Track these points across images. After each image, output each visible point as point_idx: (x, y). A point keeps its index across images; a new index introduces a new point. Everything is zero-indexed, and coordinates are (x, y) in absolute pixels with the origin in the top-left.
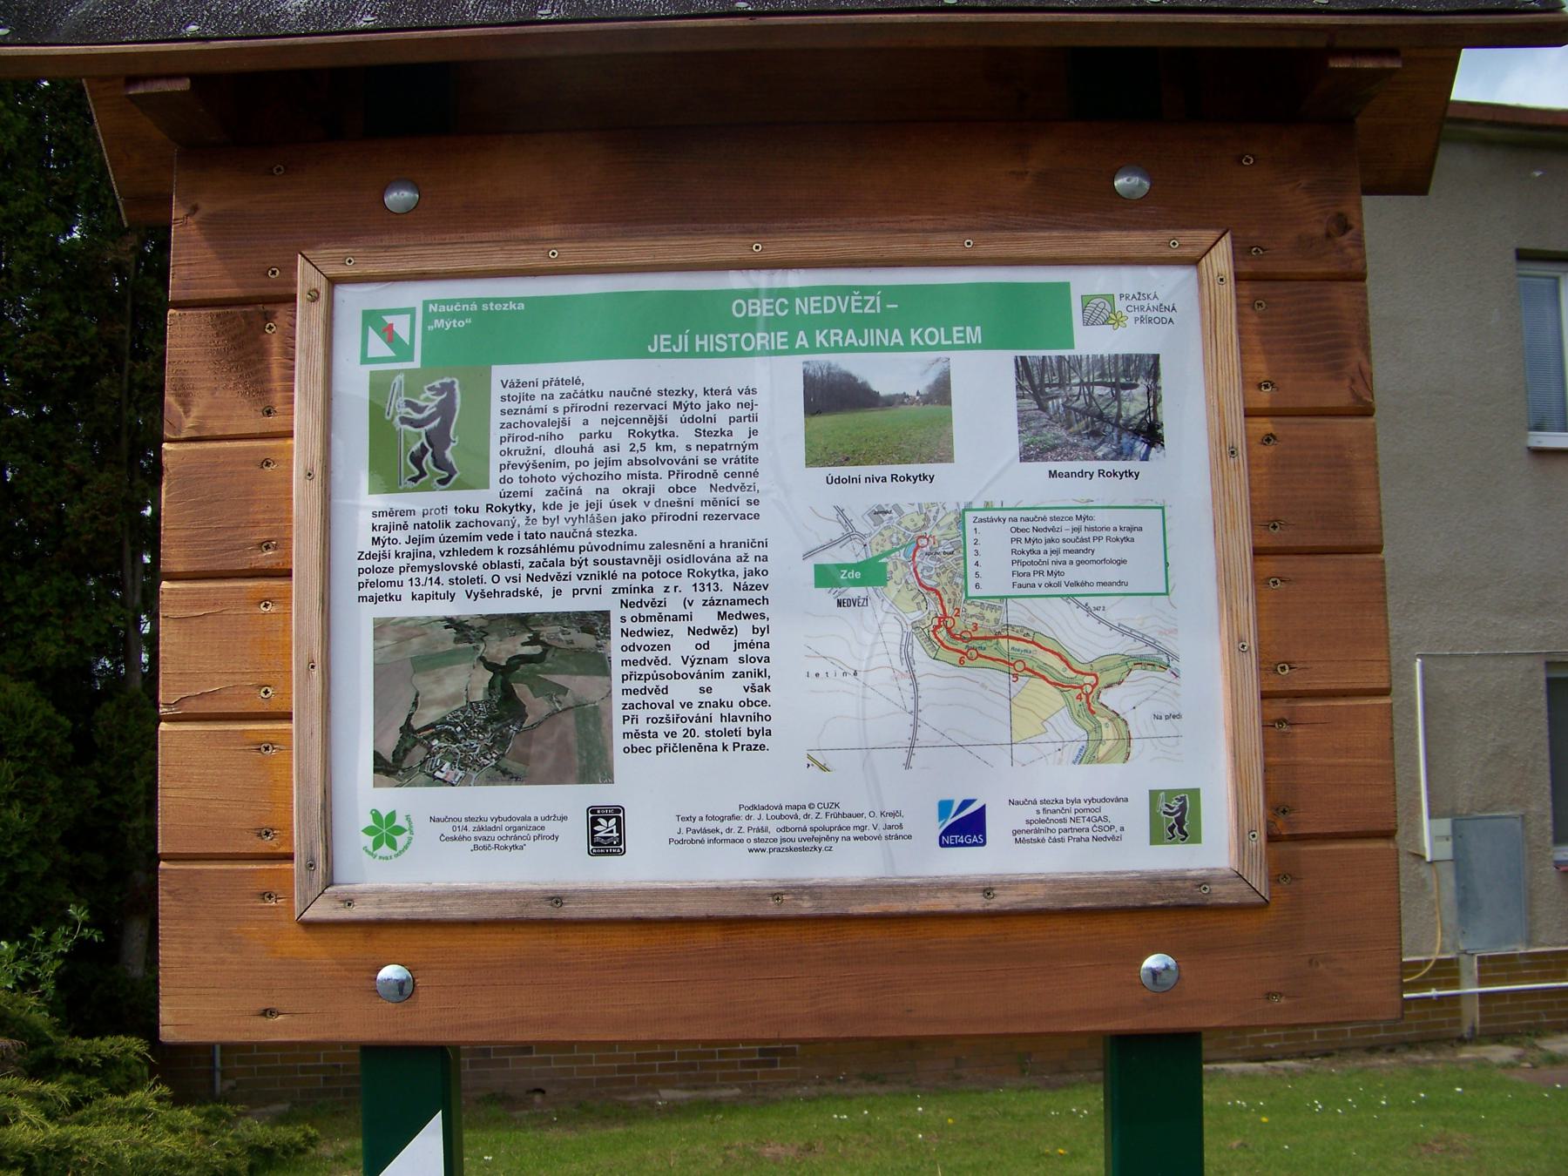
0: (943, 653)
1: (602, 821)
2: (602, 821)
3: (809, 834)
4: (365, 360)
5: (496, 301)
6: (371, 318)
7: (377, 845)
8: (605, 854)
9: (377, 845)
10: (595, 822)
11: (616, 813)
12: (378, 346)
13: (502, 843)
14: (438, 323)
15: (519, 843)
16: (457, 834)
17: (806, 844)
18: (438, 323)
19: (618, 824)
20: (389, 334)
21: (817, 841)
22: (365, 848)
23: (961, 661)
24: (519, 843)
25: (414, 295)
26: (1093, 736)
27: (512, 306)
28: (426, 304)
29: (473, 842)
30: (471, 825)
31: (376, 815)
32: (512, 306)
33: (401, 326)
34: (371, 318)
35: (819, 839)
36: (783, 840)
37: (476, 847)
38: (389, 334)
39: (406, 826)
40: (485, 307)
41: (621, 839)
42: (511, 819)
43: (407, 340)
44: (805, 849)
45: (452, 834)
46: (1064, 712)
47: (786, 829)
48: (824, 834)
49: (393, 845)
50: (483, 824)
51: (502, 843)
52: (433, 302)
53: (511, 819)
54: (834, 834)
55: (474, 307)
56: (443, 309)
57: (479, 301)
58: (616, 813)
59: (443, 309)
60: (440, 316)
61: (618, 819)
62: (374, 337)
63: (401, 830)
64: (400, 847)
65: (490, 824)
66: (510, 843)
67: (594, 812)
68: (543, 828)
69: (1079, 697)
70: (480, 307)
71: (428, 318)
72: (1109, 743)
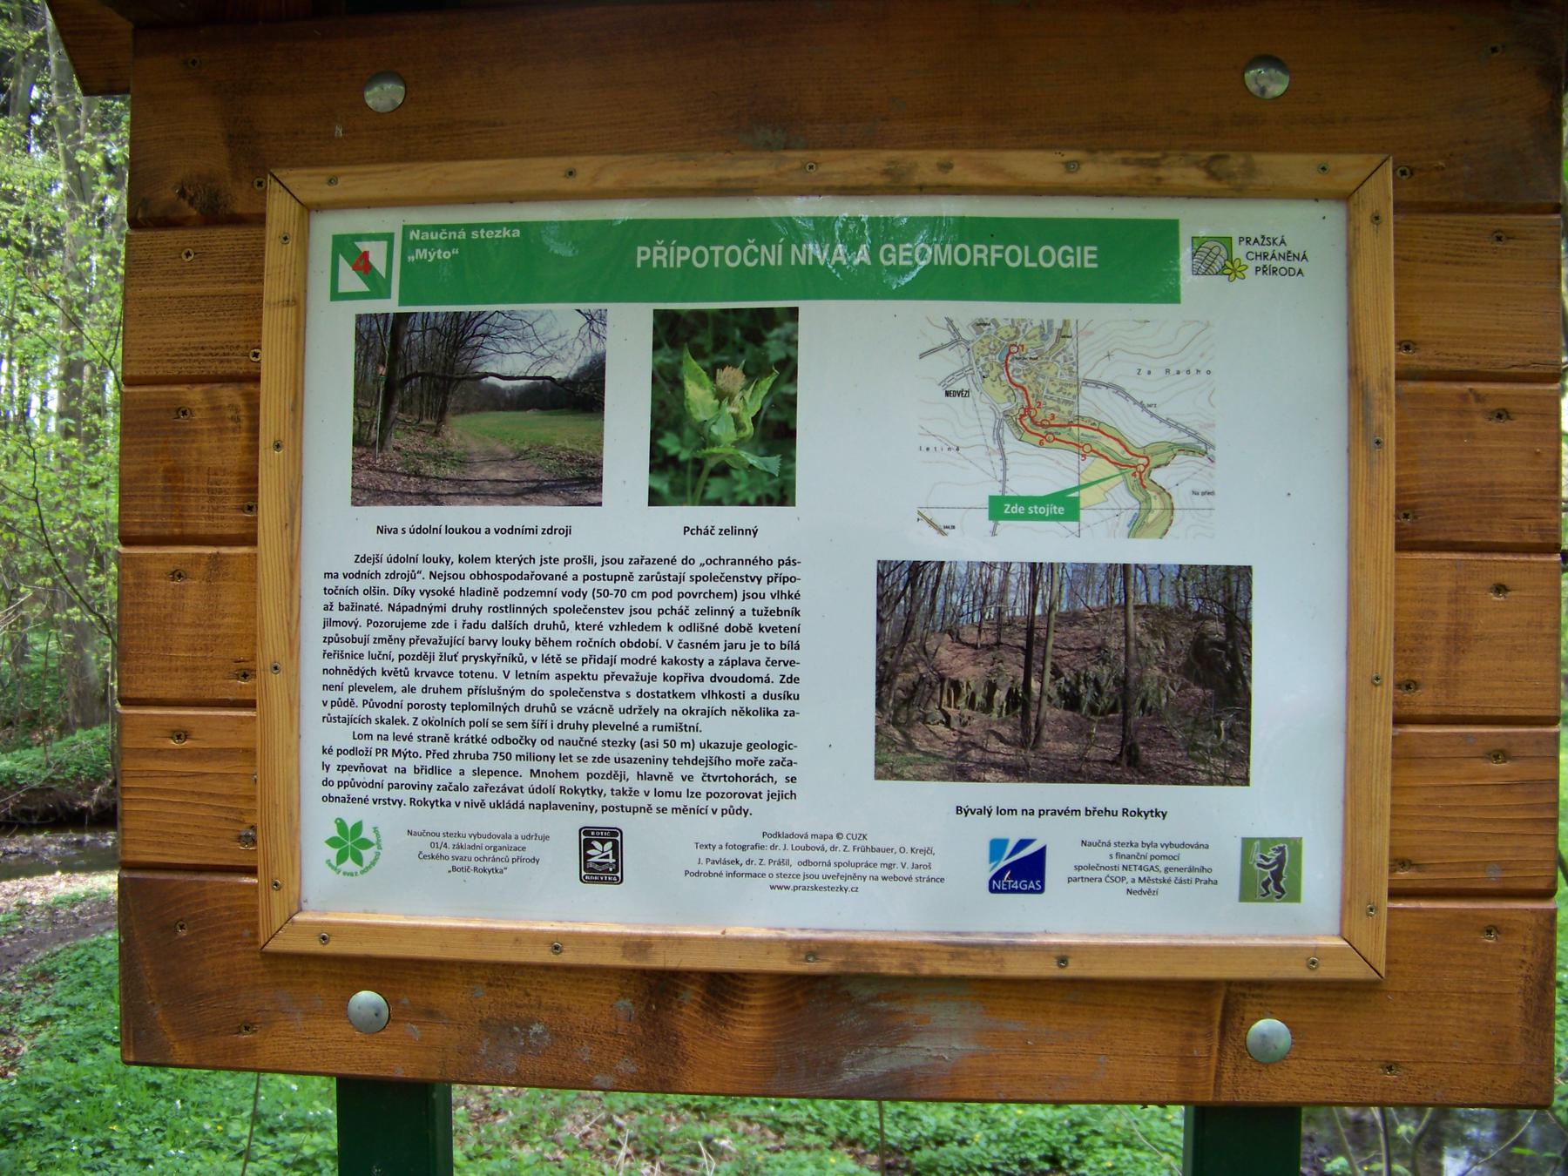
1: (596, 844)
2: (596, 844)
3: (832, 870)
4: (336, 295)
5: (487, 226)
6: (343, 245)
7: (341, 858)
8: (599, 881)
9: (341, 858)
10: (587, 845)
11: (613, 836)
12: (351, 280)
13: (480, 865)
14: (421, 254)
15: (499, 865)
16: (435, 852)
17: (831, 883)
18: (421, 254)
19: (615, 848)
20: (363, 265)
21: (845, 880)
24: (499, 865)
25: (390, 221)
27: (506, 233)
28: (406, 229)
29: (449, 864)
30: (450, 841)
34: (343, 245)
35: (845, 877)
36: (806, 876)
37: (454, 869)
38: (363, 265)
39: (373, 839)
40: (475, 235)
41: (618, 866)
42: (490, 836)
43: (382, 270)
45: (428, 851)
47: (807, 863)
48: (850, 871)
52: (415, 227)
53: (490, 836)
54: (862, 871)
55: (463, 235)
57: (469, 228)
58: (613, 836)
61: (615, 843)
62: (345, 267)
63: (367, 844)
64: (366, 863)
65: (470, 841)
66: (490, 865)
70: (469, 235)
71: (409, 246)
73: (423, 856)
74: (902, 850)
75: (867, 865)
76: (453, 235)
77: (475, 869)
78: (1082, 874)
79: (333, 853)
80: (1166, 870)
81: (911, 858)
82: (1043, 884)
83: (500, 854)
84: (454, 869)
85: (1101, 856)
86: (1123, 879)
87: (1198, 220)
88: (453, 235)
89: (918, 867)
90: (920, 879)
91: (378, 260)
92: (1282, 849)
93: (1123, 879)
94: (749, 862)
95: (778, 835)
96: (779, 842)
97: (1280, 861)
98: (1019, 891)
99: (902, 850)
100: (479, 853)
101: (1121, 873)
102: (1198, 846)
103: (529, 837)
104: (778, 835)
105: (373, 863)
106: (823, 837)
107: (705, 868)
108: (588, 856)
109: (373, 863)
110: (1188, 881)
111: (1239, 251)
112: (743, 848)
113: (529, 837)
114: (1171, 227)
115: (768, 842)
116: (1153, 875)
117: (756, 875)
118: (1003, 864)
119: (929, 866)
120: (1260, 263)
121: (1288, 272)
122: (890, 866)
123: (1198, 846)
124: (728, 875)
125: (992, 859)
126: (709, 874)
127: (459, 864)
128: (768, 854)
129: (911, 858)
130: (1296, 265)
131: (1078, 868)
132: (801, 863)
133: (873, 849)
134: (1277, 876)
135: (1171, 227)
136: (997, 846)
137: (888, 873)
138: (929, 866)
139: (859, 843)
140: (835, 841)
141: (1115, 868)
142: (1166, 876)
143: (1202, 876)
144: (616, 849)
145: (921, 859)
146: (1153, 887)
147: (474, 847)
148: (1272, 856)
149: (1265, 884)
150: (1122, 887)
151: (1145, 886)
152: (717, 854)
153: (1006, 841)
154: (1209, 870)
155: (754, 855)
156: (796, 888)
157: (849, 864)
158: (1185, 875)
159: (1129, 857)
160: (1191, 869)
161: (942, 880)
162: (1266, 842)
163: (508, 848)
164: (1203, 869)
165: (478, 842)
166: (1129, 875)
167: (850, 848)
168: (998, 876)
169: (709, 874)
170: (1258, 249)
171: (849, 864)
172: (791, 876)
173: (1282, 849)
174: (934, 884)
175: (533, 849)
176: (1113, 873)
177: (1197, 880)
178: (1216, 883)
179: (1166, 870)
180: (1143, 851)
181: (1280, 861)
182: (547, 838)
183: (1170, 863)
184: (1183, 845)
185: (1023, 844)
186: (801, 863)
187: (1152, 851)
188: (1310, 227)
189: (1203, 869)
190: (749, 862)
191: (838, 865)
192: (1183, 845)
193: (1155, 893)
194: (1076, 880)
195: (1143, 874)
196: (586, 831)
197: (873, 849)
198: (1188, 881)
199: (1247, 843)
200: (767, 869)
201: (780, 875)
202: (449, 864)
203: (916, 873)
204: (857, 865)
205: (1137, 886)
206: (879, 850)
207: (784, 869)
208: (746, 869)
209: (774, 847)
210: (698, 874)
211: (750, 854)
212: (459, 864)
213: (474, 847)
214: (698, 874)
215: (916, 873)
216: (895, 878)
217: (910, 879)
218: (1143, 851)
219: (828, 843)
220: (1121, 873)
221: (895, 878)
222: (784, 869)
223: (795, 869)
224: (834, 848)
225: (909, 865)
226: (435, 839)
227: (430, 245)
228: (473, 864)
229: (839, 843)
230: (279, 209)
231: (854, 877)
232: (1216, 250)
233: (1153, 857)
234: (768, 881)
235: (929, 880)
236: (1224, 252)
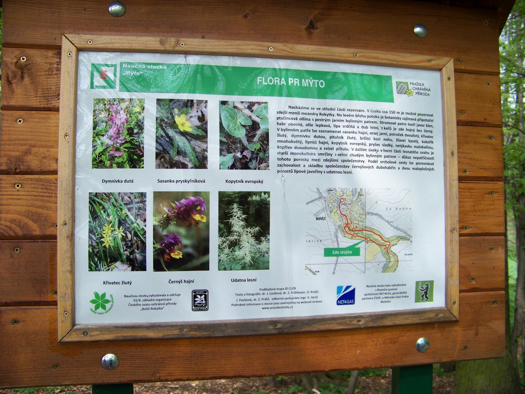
0: (347, 235)
1: (198, 296)
2: (198, 296)
3: (284, 301)
7: (97, 308)
8: (199, 310)
9: (97, 308)
10: (195, 297)
11: (205, 293)
13: (153, 307)
15: (161, 306)
16: (135, 303)
19: (205, 298)
22: (91, 310)
23: (352, 237)
24: (161, 306)
26: (388, 260)
30: (142, 299)
31: (97, 295)
35: (288, 303)
37: (143, 309)
39: (110, 299)
41: (206, 304)
42: (158, 295)
45: (133, 303)
46: (381, 253)
47: (275, 299)
49: (104, 308)
50: (146, 298)
51: (153, 307)
53: (158, 295)
54: (294, 300)
58: (205, 293)
61: (206, 295)
63: (108, 301)
64: (107, 309)
65: (150, 298)
66: (157, 307)
67: (195, 292)
68: (171, 299)
69: (385, 249)
72: (392, 263)
73: (130, 305)
74: (308, 292)
75: (296, 298)
77: (152, 308)
78: (367, 297)
79: (93, 306)
80: (393, 294)
81: (311, 295)
82: (354, 301)
83: (161, 302)
84: (143, 309)
85: (372, 290)
86: (379, 298)
87: (399, 76)
89: (313, 298)
90: (314, 302)
92: (428, 284)
93: (379, 298)
95: (265, 289)
96: (265, 292)
97: (427, 288)
98: (347, 304)
99: (308, 292)
100: (153, 302)
101: (379, 296)
102: (403, 285)
103: (173, 295)
104: (265, 289)
105: (110, 309)
106: (281, 289)
107: (239, 303)
108: (195, 301)
109: (110, 309)
110: (400, 297)
111: (411, 87)
112: (253, 295)
113: (173, 295)
114: (389, 78)
115: (261, 292)
116: (389, 296)
117: (257, 304)
118: (341, 295)
119: (317, 297)
120: (417, 91)
121: (425, 94)
122: (304, 298)
124: (247, 305)
125: (338, 294)
126: (241, 305)
127: (145, 307)
128: (261, 296)
129: (311, 295)
130: (427, 92)
131: (365, 295)
132: (273, 299)
133: (298, 293)
134: (426, 293)
135: (389, 78)
136: (339, 289)
137: (303, 300)
138: (317, 297)
140: (285, 290)
141: (377, 294)
142: (393, 296)
143: (404, 295)
145: (314, 295)
146: (389, 300)
147: (151, 300)
148: (425, 286)
149: (423, 296)
150: (380, 300)
151: (387, 300)
152: (243, 298)
153: (342, 287)
154: (406, 293)
156: (271, 308)
157: (290, 298)
158: (399, 295)
159: (382, 290)
160: (401, 293)
161: (321, 302)
162: (423, 282)
164: (404, 293)
165: (153, 298)
166: (381, 296)
167: (290, 293)
168: (339, 299)
169: (241, 305)
170: (415, 86)
171: (290, 298)
172: (269, 304)
173: (428, 284)
174: (318, 303)
175: (174, 299)
176: (377, 296)
177: (403, 296)
178: (408, 297)
179: (393, 294)
180: (386, 288)
181: (427, 288)
182: (180, 295)
183: (395, 291)
184: (398, 285)
185: (348, 287)
186: (273, 299)
187: (389, 288)
188: (430, 79)
189: (404, 293)
190: (255, 300)
191: (286, 299)
192: (398, 285)
193: (390, 302)
194: (365, 299)
195: (386, 296)
196: (194, 292)
197: (298, 293)
198: (400, 297)
199: (417, 283)
201: (266, 304)
202: (142, 307)
203: (313, 300)
204: (292, 299)
205: (384, 300)
206: (300, 293)
207: (267, 302)
208: (254, 302)
209: (264, 294)
210: (237, 305)
212: (145, 307)
213: (151, 300)
214: (237, 305)
215: (313, 300)
216: (306, 302)
217: (310, 302)
218: (386, 288)
219: (282, 291)
220: (379, 296)
221: (306, 302)
222: (267, 302)
223: (271, 301)
224: (284, 293)
225: (310, 297)
226: (136, 298)
228: (150, 307)
231: (292, 303)
232: (404, 86)
233: (389, 290)
235: (317, 302)
236: (406, 87)
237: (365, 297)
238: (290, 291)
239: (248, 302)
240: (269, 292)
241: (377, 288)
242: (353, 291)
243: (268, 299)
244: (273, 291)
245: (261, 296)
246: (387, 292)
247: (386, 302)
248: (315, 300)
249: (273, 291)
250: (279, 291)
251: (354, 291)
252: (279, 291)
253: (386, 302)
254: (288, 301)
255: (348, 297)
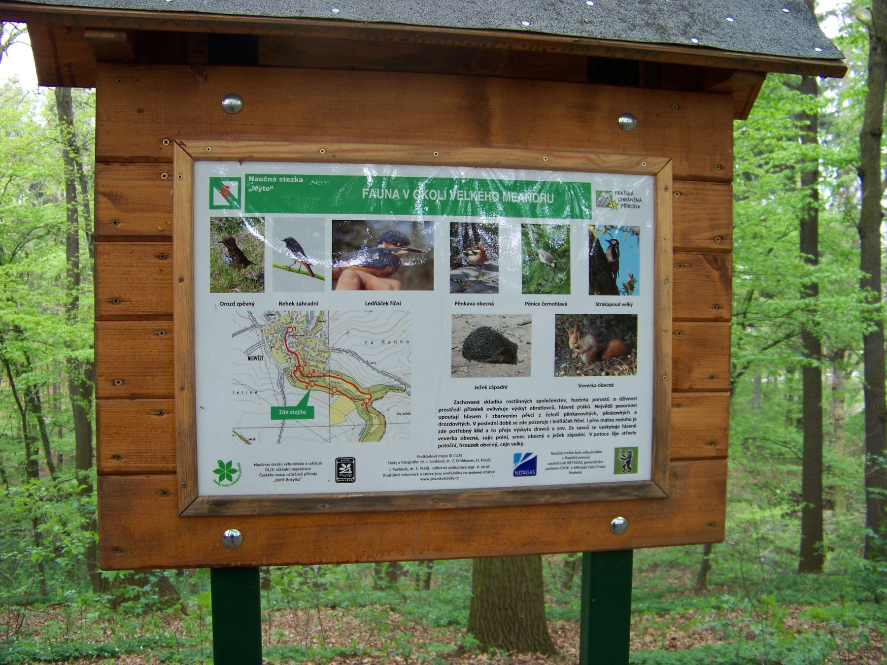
2: (343, 465)
3: (448, 471)
7: (221, 479)
8: (344, 482)
9: (221, 479)
10: (339, 466)
11: (351, 461)
12: (219, 200)
13: (289, 477)
15: (298, 477)
16: (268, 473)
17: (447, 476)
18: (255, 188)
19: (352, 467)
20: (225, 192)
24: (298, 477)
27: (296, 180)
28: (247, 176)
29: (274, 478)
30: (275, 467)
31: (221, 463)
32: (296, 180)
33: (233, 186)
34: (216, 182)
37: (277, 480)
38: (225, 192)
39: (237, 468)
40: (281, 180)
41: (353, 475)
42: (294, 464)
44: (446, 478)
45: (264, 473)
47: (437, 468)
48: (455, 470)
49: (230, 478)
50: (280, 467)
52: (251, 175)
53: (294, 464)
54: (460, 470)
55: (275, 180)
56: (257, 180)
57: (278, 176)
58: (351, 461)
59: (257, 180)
60: (255, 184)
61: (352, 464)
62: (217, 192)
63: (234, 471)
64: (234, 480)
65: (285, 467)
66: (294, 477)
70: (278, 180)
73: (261, 475)
76: (270, 179)
78: (552, 466)
81: (481, 464)
84: (277, 480)
85: (558, 458)
88: (270, 179)
90: (484, 472)
91: (234, 192)
94: (412, 469)
95: (424, 456)
96: (424, 459)
97: (630, 456)
99: (478, 460)
100: (288, 472)
102: (598, 452)
104: (424, 456)
107: (392, 473)
110: (594, 467)
115: (419, 459)
116: (580, 465)
118: (519, 464)
123: (598, 452)
127: (279, 478)
128: (419, 465)
129: (481, 464)
131: (550, 464)
133: (464, 461)
134: (628, 463)
136: (517, 457)
137: (472, 471)
139: (459, 458)
143: (600, 465)
144: (352, 467)
145: (485, 464)
146: (580, 470)
147: (287, 469)
148: (626, 455)
149: (624, 467)
150: (567, 471)
151: (577, 470)
155: (413, 465)
156: (432, 479)
158: (593, 465)
160: (595, 462)
162: (624, 449)
163: (302, 469)
164: (599, 462)
165: (288, 467)
168: (517, 469)
180: (575, 455)
181: (630, 456)
183: (587, 460)
184: (592, 452)
185: (528, 455)
187: (579, 455)
189: (599, 462)
190: (412, 469)
191: (450, 468)
192: (592, 452)
195: (576, 465)
196: (339, 459)
197: (464, 461)
198: (594, 467)
199: (617, 450)
200: (419, 471)
202: (274, 478)
204: (458, 468)
205: (573, 470)
207: (427, 471)
208: (411, 472)
209: (422, 462)
211: (412, 465)
212: (279, 478)
213: (287, 469)
216: (474, 473)
218: (575, 455)
219: (445, 459)
221: (474, 473)
222: (427, 471)
224: (448, 461)
227: (260, 184)
228: (286, 477)
229: (450, 459)
230: (181, 163)
234: (420, 477)
237: (549, 467)
238: (455, 459)
239: (404, 472)
240: (429, 459)
241: (564, 456)
242: (534, 460)
243: (428, 468)
244: (434, 459)
245: (419, 465)
246: (577, 460)
247: (575, 473)
248: (485, 469)
249: (434, 459)
250: (441, 459)
251: (535, 458)
252: (441, 459)
253: (575, 473)
254: (452, 470)
255: (528, 466)
